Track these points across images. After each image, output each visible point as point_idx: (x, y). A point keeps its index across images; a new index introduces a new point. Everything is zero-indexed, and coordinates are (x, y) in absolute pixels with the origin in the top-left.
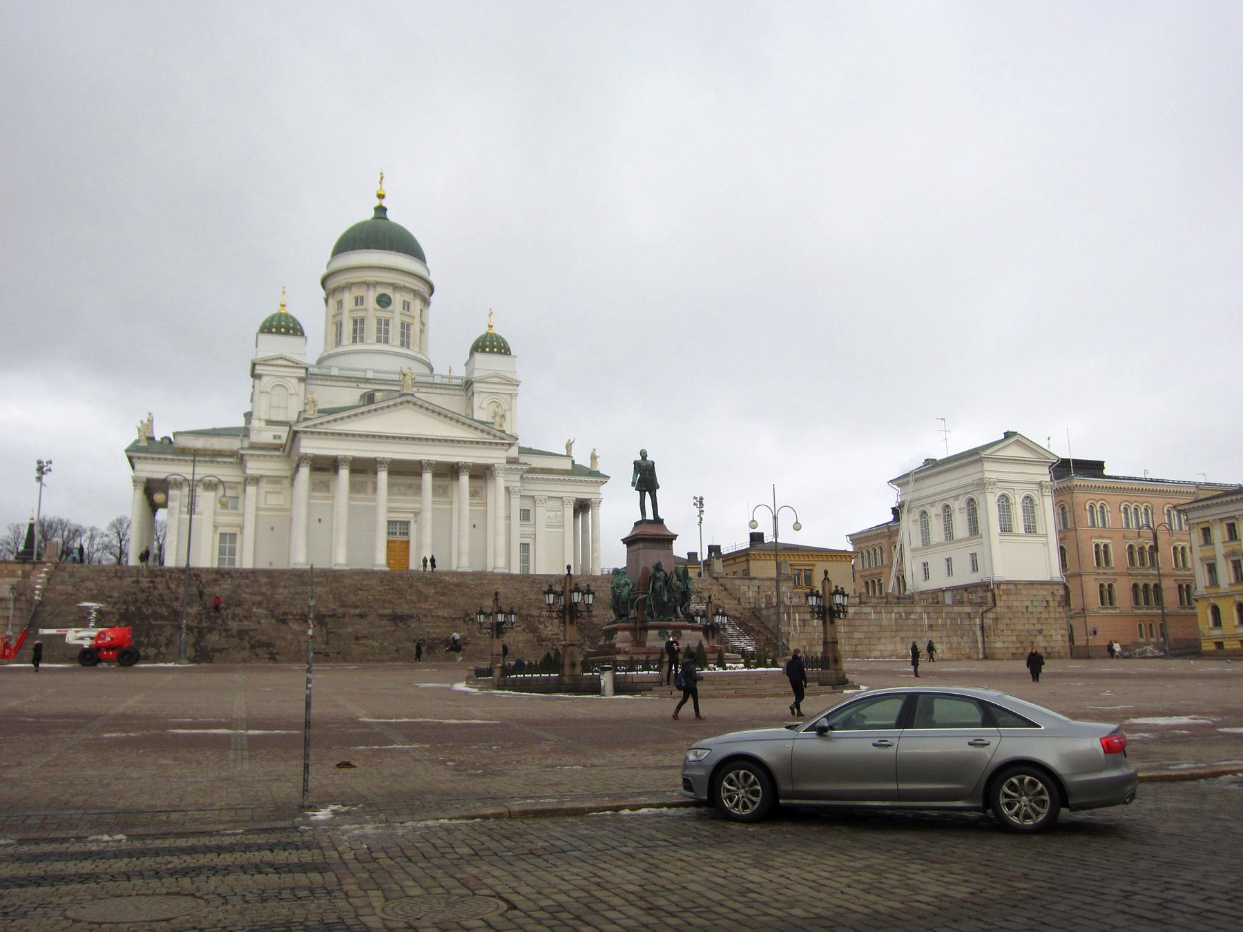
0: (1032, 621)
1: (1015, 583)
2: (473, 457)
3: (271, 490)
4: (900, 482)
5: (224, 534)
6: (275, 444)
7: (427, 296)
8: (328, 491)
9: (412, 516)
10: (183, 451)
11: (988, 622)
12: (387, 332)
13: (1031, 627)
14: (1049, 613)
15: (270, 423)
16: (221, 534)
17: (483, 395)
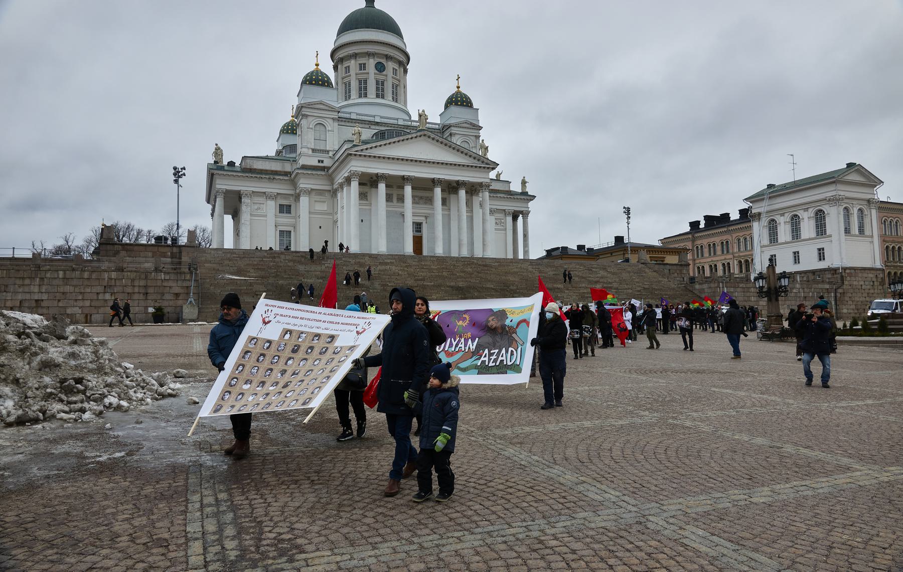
0: (863, 295)
1: (854, 269)
2: (469, 177)
3: (318, 200)
4: (751, 199)
5: (282, 231)
6: (319, 166)
7: (406, 65)
8: (367, 200)
9: (424, 218)
10: (251, 171)
11: (838, 295)
12: (383, 90)
13: (864, 299)
14: (874, 289)
15: (314, 150)
16: (280, 231)
17: (457, 137)
